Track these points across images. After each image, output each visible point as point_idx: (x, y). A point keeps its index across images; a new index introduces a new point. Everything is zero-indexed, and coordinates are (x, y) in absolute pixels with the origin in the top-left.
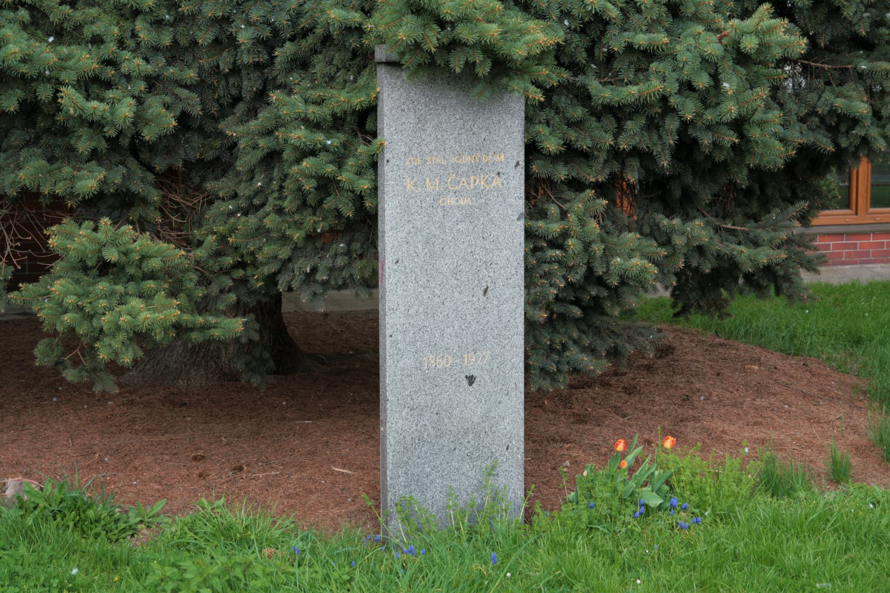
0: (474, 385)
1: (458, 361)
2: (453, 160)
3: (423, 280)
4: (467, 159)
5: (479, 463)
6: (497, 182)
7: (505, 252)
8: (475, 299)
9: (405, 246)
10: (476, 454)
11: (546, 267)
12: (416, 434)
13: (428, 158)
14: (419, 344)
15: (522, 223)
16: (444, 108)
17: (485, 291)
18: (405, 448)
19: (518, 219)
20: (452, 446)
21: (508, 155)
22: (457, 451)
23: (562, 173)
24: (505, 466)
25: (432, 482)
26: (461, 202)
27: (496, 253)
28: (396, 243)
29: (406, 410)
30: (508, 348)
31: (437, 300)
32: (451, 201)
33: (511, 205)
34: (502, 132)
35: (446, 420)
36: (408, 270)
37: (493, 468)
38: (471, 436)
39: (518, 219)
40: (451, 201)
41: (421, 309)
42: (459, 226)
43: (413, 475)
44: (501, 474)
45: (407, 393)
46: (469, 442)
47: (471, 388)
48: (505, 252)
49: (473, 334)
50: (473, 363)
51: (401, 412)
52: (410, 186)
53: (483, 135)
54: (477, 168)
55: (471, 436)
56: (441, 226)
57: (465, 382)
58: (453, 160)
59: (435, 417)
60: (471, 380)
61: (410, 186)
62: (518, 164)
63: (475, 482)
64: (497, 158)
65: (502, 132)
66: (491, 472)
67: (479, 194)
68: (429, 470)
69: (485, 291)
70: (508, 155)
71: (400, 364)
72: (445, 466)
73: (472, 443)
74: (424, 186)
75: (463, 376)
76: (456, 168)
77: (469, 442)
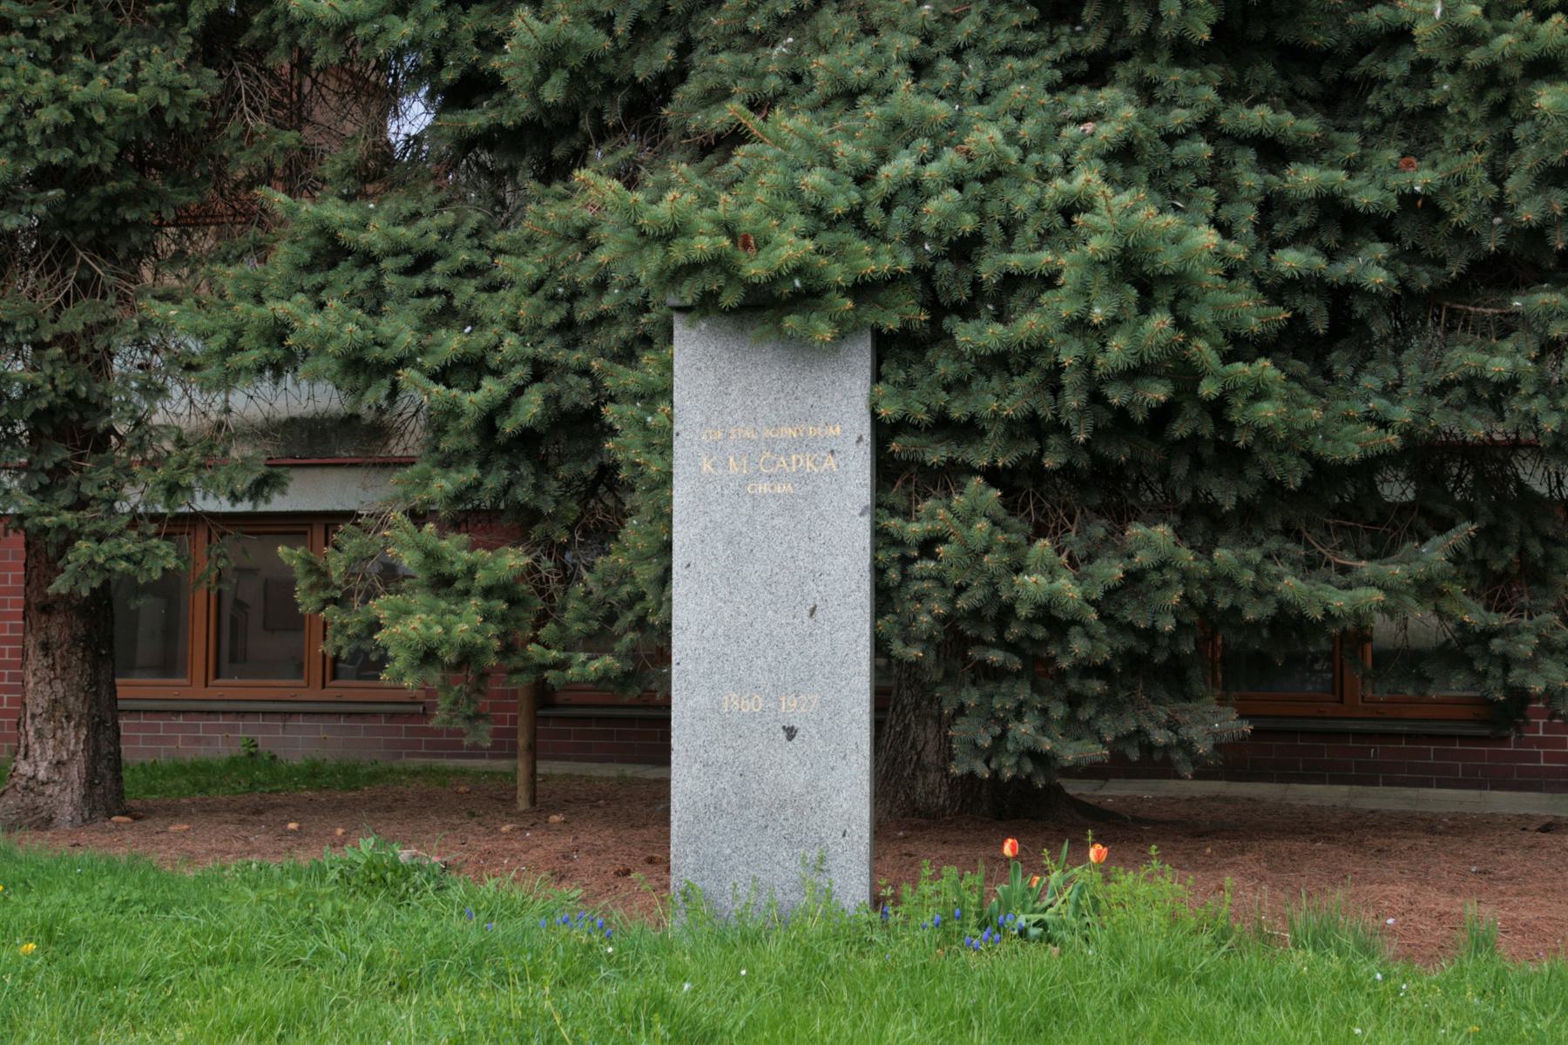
0: (795, 740)
1: (772, 705)
2: (768, 433)
3: (723, 592)
4: (789, 432)
5: (802, 850)
6: (831, 463)
7: (841, 559)
8: (797, 621)
9: (699, 546)
10: (797, 838)
11: (916, 587)
12: (711, 800)
13: (732, 431)
14: (717, 677)
15: (866, 521)
16: (755, 365)
17: (813, 611)
18: (696, 817)
19: (861, 514)
20: (762, 822)
21: (847, 426)
22: (769, 831)
23: (936, 455)
24: (841, 860)
25: (733, 869)
26: (779, 490)
27: (829, 559)
28: (687, 542)
29: (697, 766)
30: (845, 692)
31: (743, 619)
32: (763, 488)
33: (850, 496)
34: (838, 396)
35: (754, 785)
36: (703, 578)
37: (822, 860)
38: (790, 811)
39: (861, 514)
40: (763, 488)
41: (720, 631)
42: (775, 522)
43: (705, 856)
44: (834, 869)
45: (700, 742)
46: (786, 819)
47: (790, 744)
48: (841, 559)
49: (793, 669)
50: (792, 709)
51: (690, 767)
52: (707, 467)
53: (810, 402)
54: (802, 444)
55: (790, 811)
56: (750, 521)
57: (782, 735)
58: (768, 433)
59: (739, 779)
60: (791, 733)
61: (707, 467)
62: (860, 439)
63: (796, 877)
64: (831, 431)
65: (838, 396)
66: (821, 865)
67: (802, 478)
68: (728, 851)
69: (813, 611)
70: (847, 426)
71: (690, 703)
72: (752, 849)
73: (791, 821)
74: (726, 466)
75: (779, 726)
76: (771, 444)
77: (786, 819)
